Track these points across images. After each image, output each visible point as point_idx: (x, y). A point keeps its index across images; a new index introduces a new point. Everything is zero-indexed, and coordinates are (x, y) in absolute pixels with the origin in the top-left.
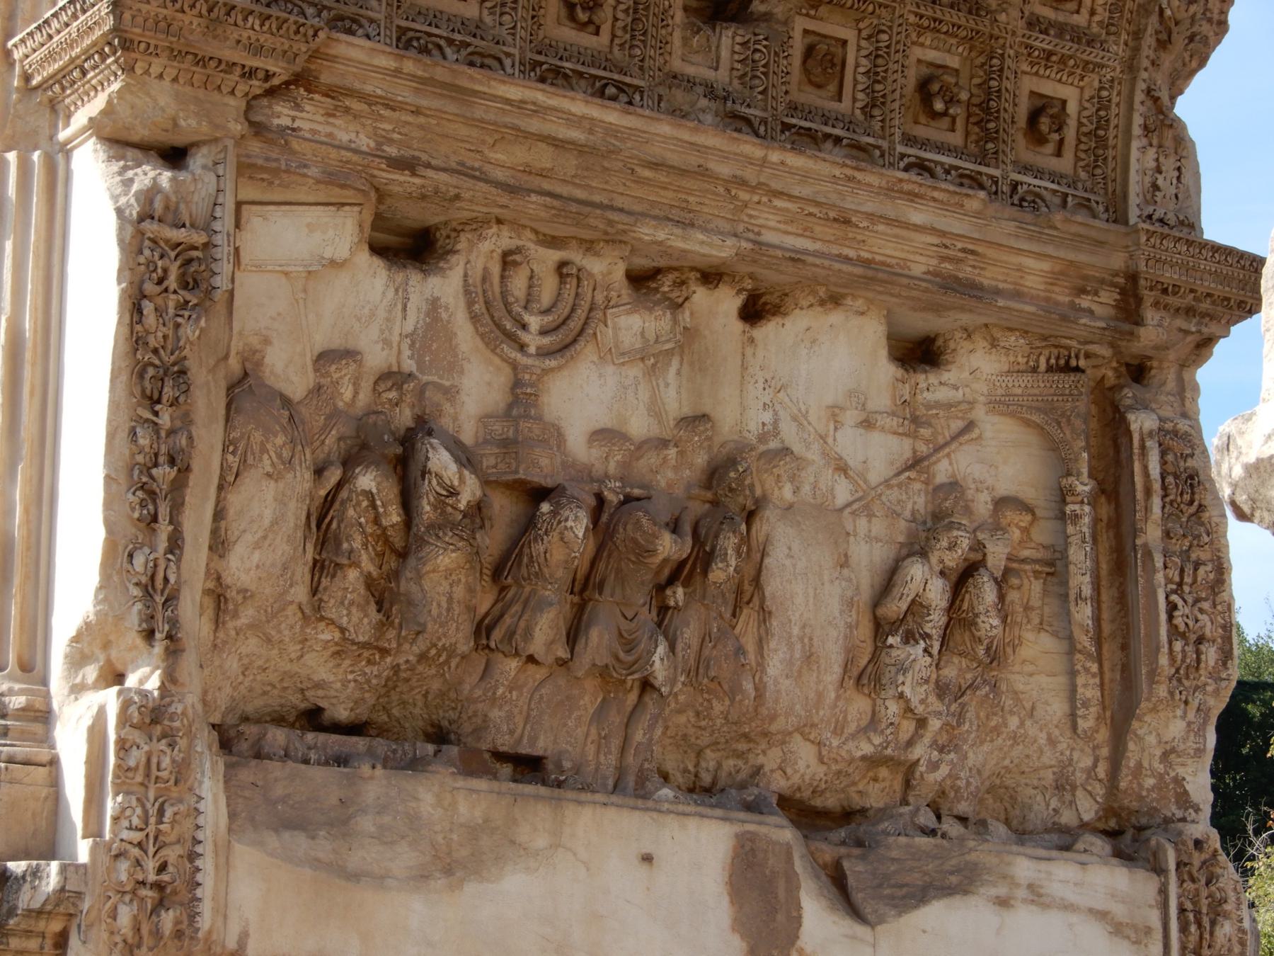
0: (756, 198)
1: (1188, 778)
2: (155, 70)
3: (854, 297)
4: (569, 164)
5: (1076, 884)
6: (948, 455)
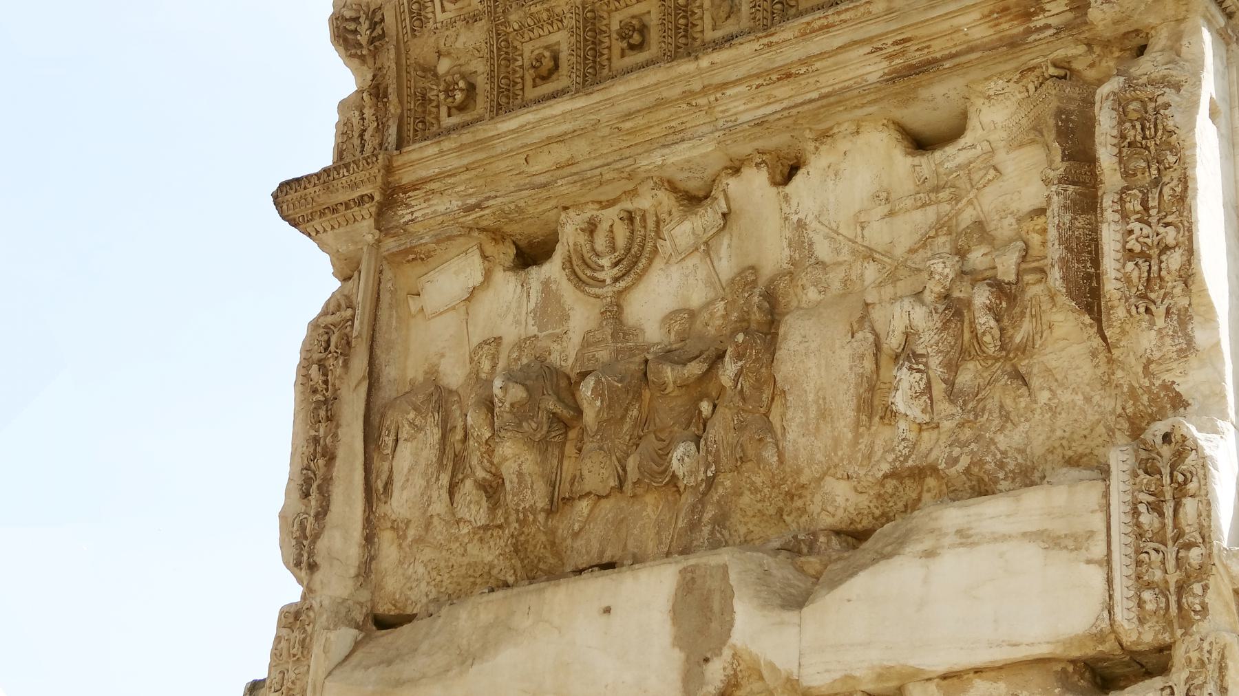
0: (712, 98)
2: (319, 228)
3: (839, 124)
4: (580, 147)
5: (1008, 516)
6: (970, 202)
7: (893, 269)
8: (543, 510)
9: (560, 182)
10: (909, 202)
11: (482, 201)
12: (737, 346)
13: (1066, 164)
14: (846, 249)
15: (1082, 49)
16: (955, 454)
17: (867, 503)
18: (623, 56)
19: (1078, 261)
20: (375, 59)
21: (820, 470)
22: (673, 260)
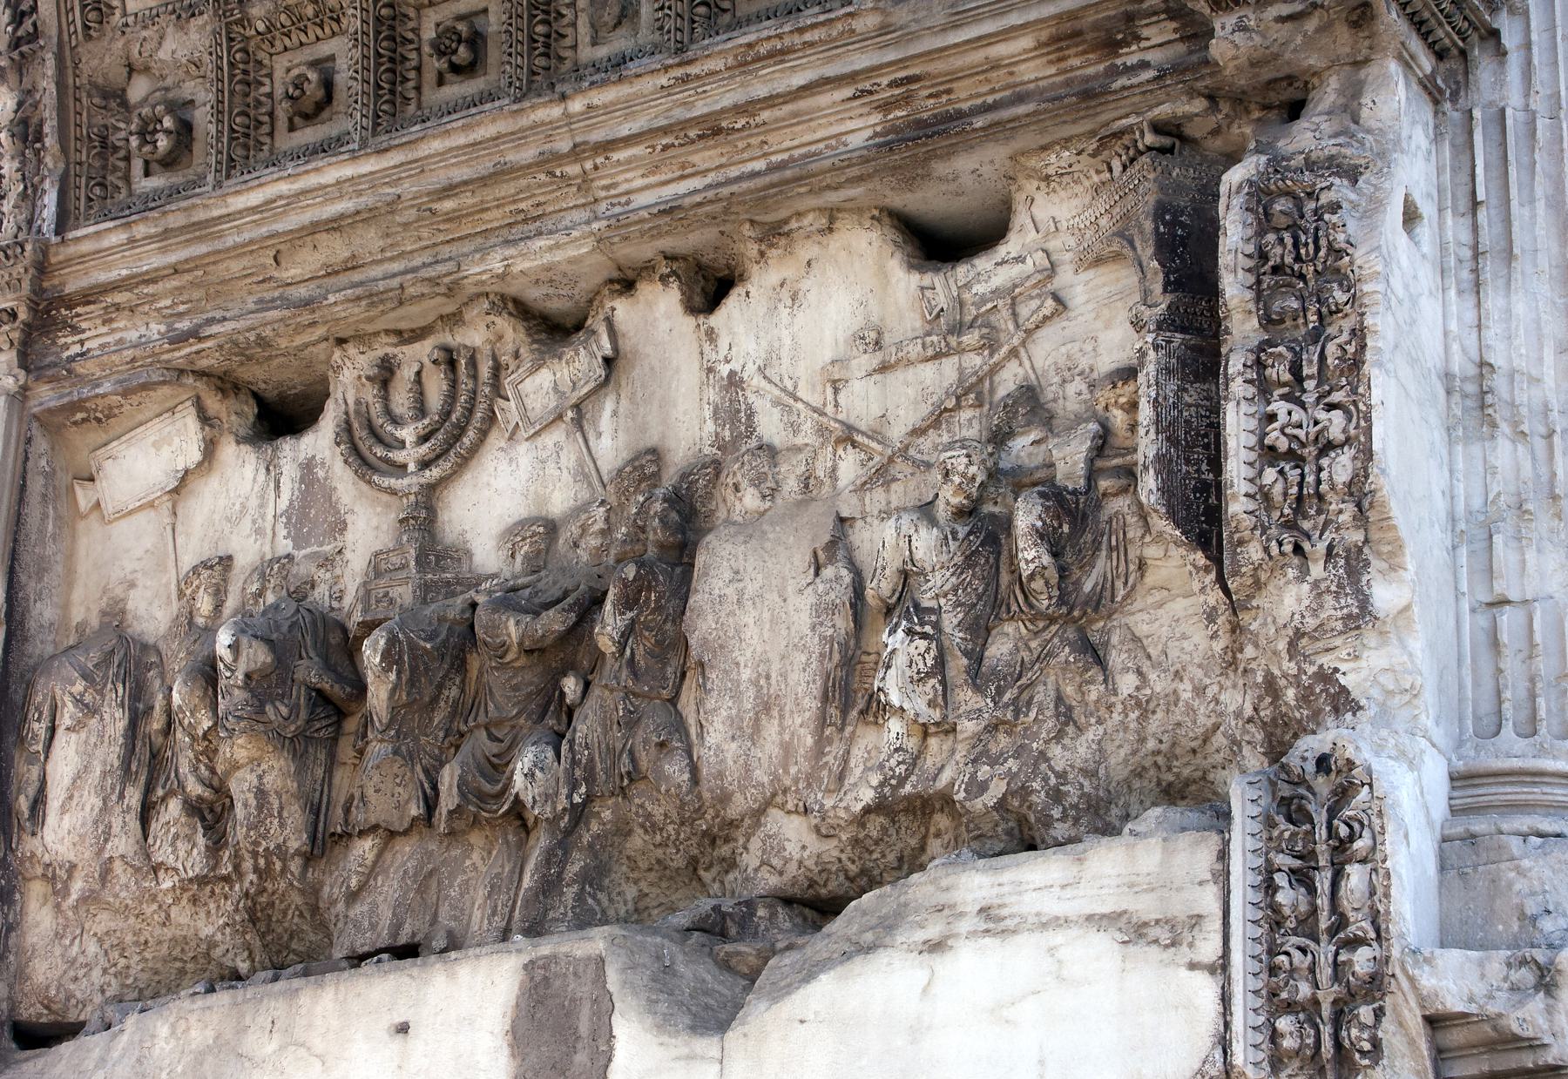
0: (589, 165)
1: (1343, 667)
4: (369, 240)
5: (1063, 887)
6: (1014, 353)
7: (885, 461)
8: (298, 852)
9: (332, 299)
10: (915, 350)
11: (200, 326)
12: (625, 586)
13: (1169, 298)
14: (809, 424)
15: (1199, 105)
16: (980, 776)
17: (836, 853)
18: (441, 82)
19: (1188, 462)
20: (21, 75)
21: (760, 797)
22: (523, 434)
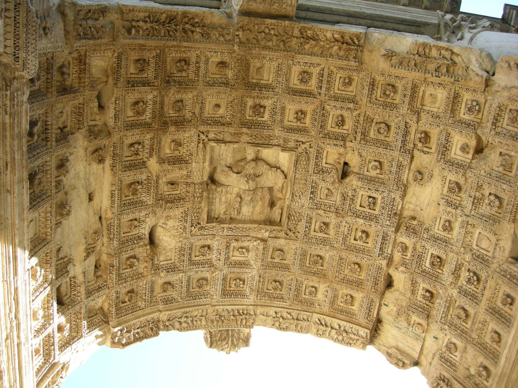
18: (511, 310)
